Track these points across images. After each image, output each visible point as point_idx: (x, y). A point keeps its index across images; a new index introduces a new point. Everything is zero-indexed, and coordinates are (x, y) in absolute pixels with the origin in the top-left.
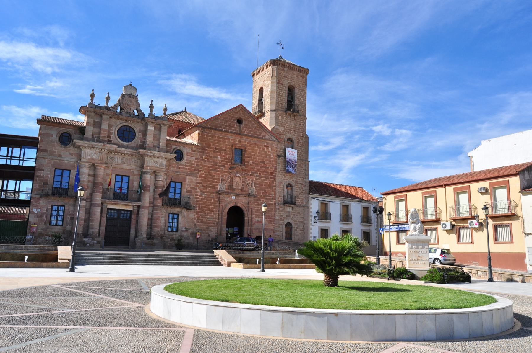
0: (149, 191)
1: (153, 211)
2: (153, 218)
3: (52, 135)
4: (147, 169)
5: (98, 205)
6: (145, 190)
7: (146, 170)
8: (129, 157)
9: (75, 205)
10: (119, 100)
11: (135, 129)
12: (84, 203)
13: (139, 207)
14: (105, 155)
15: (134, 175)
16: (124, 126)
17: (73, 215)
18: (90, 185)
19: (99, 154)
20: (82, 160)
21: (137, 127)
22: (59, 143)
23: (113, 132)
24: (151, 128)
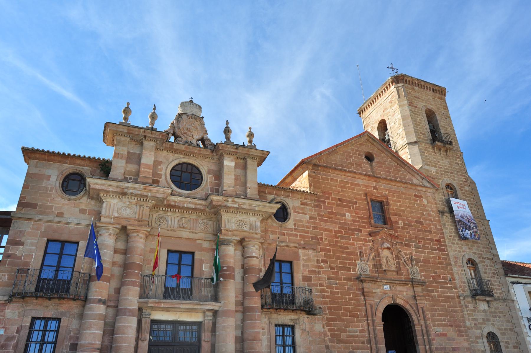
0: (233, 278)
1: (243, 321)
2: (246, 336)
3: (48, 177)
4: (228, 235)
5: (131, 313)
6: (225, 277)
7: (226, 238)
8: (193, 216)
9: (81, 316)
10: (173, 124)
11: (201, 168)
12: (100, 309)
13: (215, 313)
14: (147, 211)
15: (203, 250)
16: (182, 164)
17: (77, 338)
18: (117, 271)
19: (136, 208)
20: (103, 219)
21: (205, 166)
22: (60, 192)
23: (163, 172)
24: (229, 163)
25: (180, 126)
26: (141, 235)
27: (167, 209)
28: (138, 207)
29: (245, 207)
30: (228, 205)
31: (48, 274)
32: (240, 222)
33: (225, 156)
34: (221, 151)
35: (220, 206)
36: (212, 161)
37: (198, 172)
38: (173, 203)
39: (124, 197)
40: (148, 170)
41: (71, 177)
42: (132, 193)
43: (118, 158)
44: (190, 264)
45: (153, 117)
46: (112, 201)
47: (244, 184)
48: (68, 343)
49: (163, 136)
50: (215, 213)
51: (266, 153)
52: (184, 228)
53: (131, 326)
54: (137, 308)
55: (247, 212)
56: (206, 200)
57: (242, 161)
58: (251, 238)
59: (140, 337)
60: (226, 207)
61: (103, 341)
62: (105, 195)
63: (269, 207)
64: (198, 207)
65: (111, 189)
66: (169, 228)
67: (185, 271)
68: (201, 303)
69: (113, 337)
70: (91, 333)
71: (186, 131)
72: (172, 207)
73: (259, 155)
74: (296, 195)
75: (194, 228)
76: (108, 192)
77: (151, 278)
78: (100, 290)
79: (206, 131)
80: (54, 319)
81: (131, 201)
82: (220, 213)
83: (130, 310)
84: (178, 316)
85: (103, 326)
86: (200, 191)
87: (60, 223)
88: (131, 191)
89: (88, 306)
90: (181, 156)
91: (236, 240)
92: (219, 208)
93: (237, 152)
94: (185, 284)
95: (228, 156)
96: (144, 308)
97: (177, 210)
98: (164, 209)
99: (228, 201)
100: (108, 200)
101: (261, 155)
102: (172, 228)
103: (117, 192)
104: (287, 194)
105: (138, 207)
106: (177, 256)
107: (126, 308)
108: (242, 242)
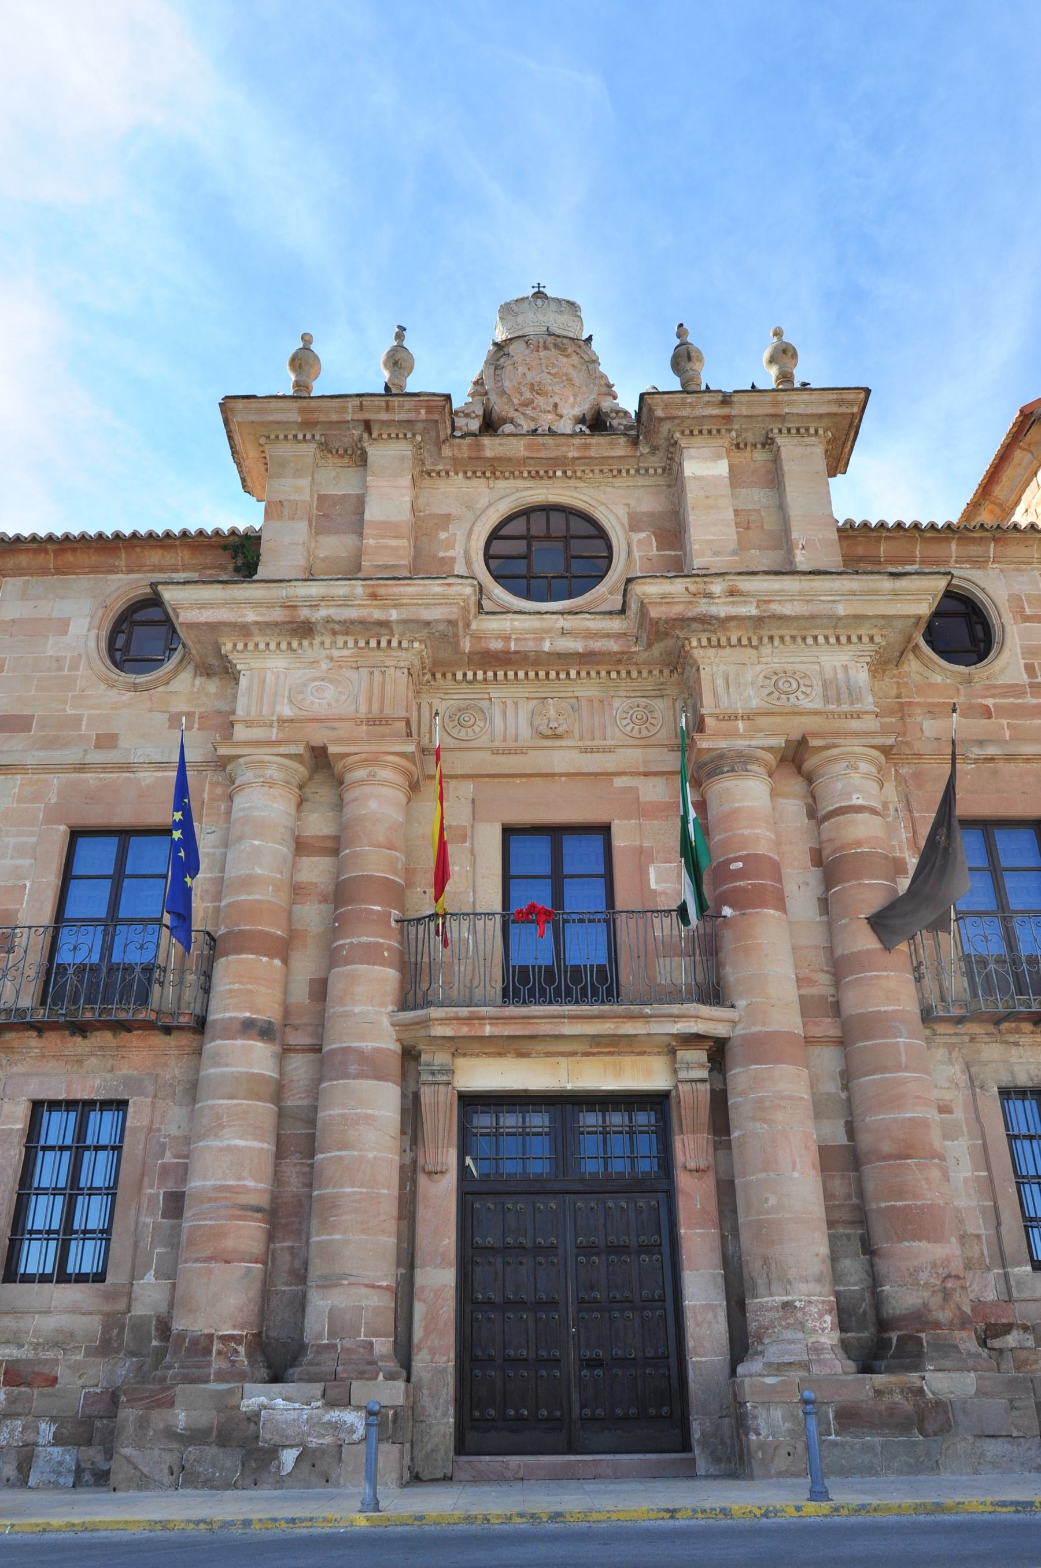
0: (780, 902)
1: (847, 1078)
2: (865, 1140)
3: (63, 626)
4: (734, 734)
5: (370, 1066)
6: (740, 900)
7: (723, 744)
8: (587, 689)
9: (193, 1090)
10: (479, 383)
11: (601, 515)
12: (256, 1058)
14: (398, 684)
15: (643, 811)
16: (527, 513)
17: (183, 1172)
18: (312, 915)
19: (358, 680)
20: (241, 733)
21: (615, 503)
22: (102, 665)
23: (457, 552)
24: (704, 467)
25: (507, 384)
26: (385, 774)
27: (480, 675)
28: (364, 672)
29: (788, 610)
30: (714, 610)
31: (81, 949)
32: (776, 681)
33: (683, 443)
34: (665, 427)
35: (683, 621)
36: (640, 481)
37: (593, 531)
38: (497, 645)
39: (305, 643)
40: (394, 543)
41: (138, 617)
42: (329, 620)
43: (280, 517)
44: (601, 869)
45: (396, 363)
46: (270, 663)
47: (782, 539)
48: (156, 1191)
49: (429, 410)
50: (667, 651)
51: (850, 396)
52: (558, 737)
53: (373, 1117)
54: (397, 1048)
55: (803, 628)
56: (623, 611)
57: (760, 456)
58: (837, 734)
59: (421, 1161)
60: (705, 621)
61: (278, 1178)
62: (240, 646)
63: (895, 593)
64: (598, 645)
65: (251, 616)
66: (497, 743)
67: (581, 897)
68: (647, 1010)
69: (312, 1166)
70: (221, 1149)
71: (528, 395)
72: (497, 661)
73: (823, 410)
74: (1016, 551)
75: (597, 734)
76: (244, 630)
77: (432, 925)
78: (246, 986)
79: (610, 386)
80: (105, 1105)
81: (336, 653)
82: (688, 655)
83: (362, 1056)
84: (563, 1073)
85: (269, 1122)
86: (605, 592)
87: (104, 768)
88: (323, 613)
89: (212, 1046)
90: (520, 483)
91: (769, 749)
92: (682, 634)
93: (728, 418)
94: (584, 949)
95: (697, 441)
96: (421, 1047)
97: (521, 674)
98: (470, 675)
99: (709, 596)
100: (254, 664)
101: (834, 409)
102: (510, 743)
103: (276, 624)
104: (974, 550)
105: (364, 672)
106: (542, 846)
107: (347, 1050)
108: (796, 759)
